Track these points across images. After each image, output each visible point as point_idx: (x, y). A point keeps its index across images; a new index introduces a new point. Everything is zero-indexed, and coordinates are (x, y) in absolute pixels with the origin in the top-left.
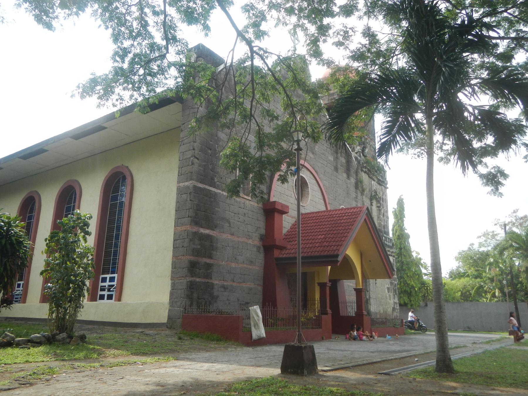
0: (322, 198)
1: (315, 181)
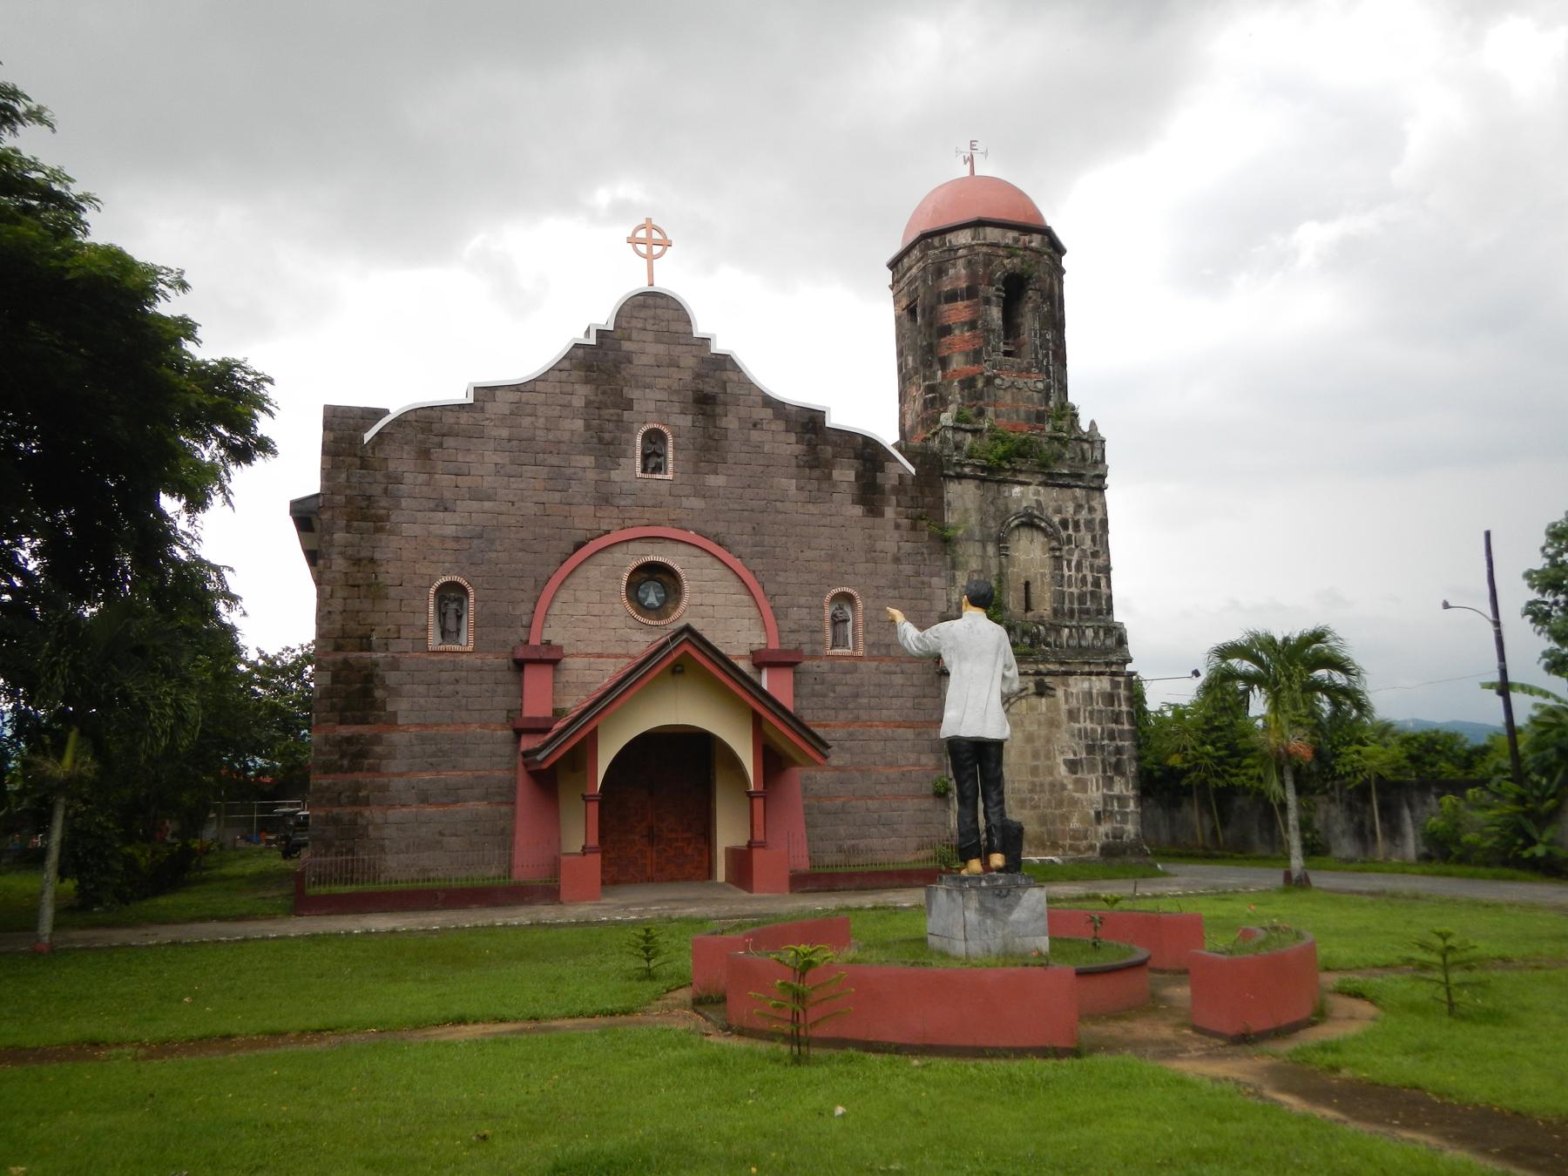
0: (743, 590)
1: (708, 560)
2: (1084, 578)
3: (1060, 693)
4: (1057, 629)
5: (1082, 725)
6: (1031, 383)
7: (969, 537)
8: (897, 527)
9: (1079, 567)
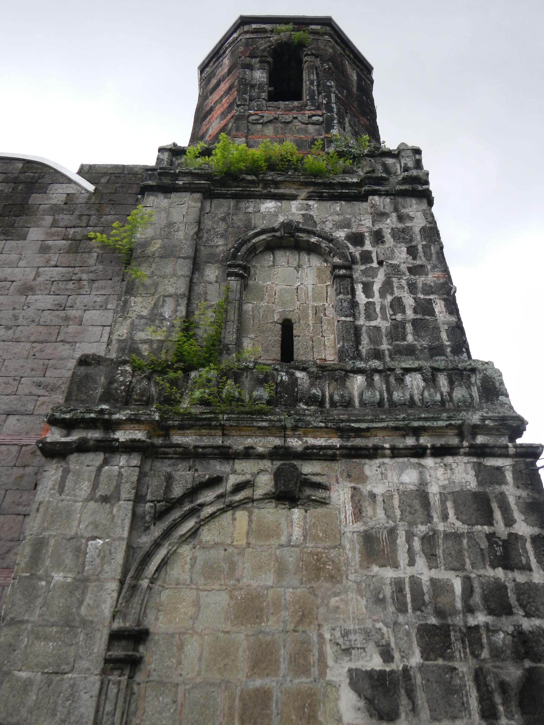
2: (398, 305)
3: (341, 495)
4: (338, 374)
5: (404, 572)
6: (304, 116)
7: (169, 253)
8: (44, 249)
9: (387, 288)
